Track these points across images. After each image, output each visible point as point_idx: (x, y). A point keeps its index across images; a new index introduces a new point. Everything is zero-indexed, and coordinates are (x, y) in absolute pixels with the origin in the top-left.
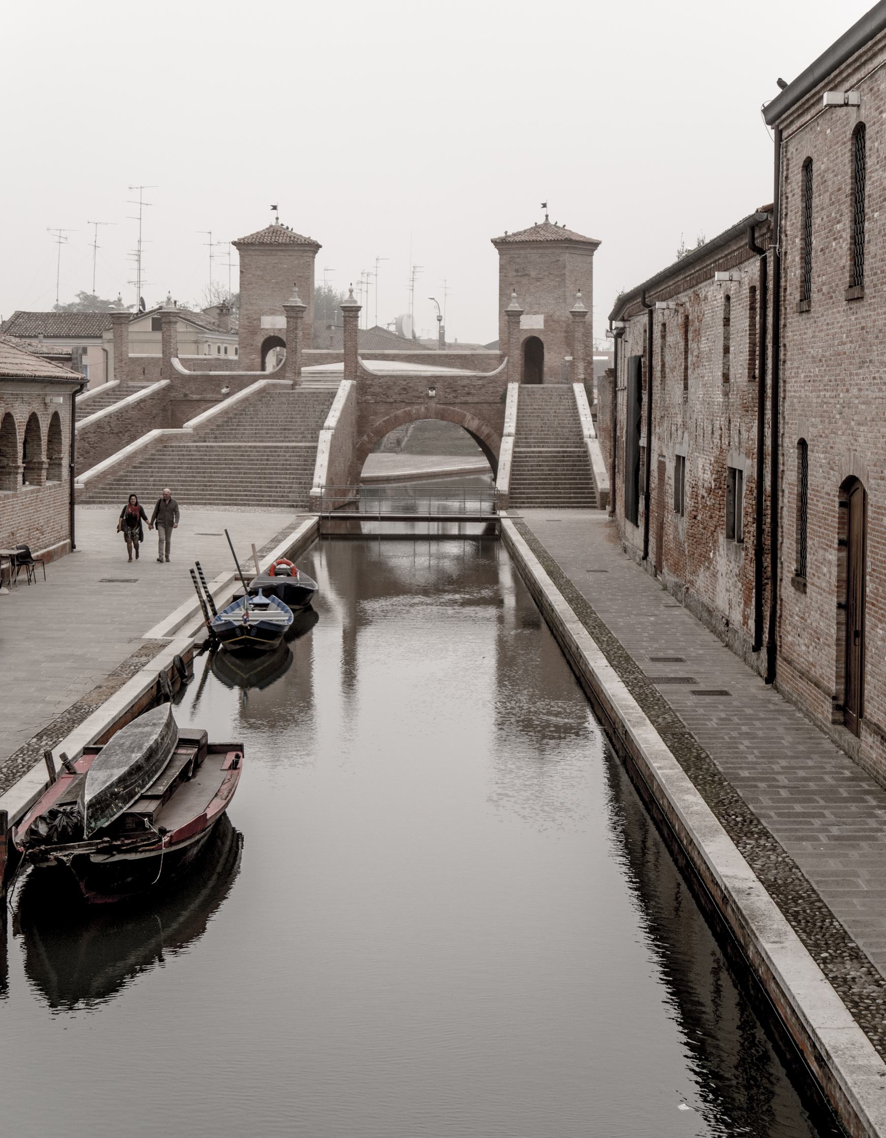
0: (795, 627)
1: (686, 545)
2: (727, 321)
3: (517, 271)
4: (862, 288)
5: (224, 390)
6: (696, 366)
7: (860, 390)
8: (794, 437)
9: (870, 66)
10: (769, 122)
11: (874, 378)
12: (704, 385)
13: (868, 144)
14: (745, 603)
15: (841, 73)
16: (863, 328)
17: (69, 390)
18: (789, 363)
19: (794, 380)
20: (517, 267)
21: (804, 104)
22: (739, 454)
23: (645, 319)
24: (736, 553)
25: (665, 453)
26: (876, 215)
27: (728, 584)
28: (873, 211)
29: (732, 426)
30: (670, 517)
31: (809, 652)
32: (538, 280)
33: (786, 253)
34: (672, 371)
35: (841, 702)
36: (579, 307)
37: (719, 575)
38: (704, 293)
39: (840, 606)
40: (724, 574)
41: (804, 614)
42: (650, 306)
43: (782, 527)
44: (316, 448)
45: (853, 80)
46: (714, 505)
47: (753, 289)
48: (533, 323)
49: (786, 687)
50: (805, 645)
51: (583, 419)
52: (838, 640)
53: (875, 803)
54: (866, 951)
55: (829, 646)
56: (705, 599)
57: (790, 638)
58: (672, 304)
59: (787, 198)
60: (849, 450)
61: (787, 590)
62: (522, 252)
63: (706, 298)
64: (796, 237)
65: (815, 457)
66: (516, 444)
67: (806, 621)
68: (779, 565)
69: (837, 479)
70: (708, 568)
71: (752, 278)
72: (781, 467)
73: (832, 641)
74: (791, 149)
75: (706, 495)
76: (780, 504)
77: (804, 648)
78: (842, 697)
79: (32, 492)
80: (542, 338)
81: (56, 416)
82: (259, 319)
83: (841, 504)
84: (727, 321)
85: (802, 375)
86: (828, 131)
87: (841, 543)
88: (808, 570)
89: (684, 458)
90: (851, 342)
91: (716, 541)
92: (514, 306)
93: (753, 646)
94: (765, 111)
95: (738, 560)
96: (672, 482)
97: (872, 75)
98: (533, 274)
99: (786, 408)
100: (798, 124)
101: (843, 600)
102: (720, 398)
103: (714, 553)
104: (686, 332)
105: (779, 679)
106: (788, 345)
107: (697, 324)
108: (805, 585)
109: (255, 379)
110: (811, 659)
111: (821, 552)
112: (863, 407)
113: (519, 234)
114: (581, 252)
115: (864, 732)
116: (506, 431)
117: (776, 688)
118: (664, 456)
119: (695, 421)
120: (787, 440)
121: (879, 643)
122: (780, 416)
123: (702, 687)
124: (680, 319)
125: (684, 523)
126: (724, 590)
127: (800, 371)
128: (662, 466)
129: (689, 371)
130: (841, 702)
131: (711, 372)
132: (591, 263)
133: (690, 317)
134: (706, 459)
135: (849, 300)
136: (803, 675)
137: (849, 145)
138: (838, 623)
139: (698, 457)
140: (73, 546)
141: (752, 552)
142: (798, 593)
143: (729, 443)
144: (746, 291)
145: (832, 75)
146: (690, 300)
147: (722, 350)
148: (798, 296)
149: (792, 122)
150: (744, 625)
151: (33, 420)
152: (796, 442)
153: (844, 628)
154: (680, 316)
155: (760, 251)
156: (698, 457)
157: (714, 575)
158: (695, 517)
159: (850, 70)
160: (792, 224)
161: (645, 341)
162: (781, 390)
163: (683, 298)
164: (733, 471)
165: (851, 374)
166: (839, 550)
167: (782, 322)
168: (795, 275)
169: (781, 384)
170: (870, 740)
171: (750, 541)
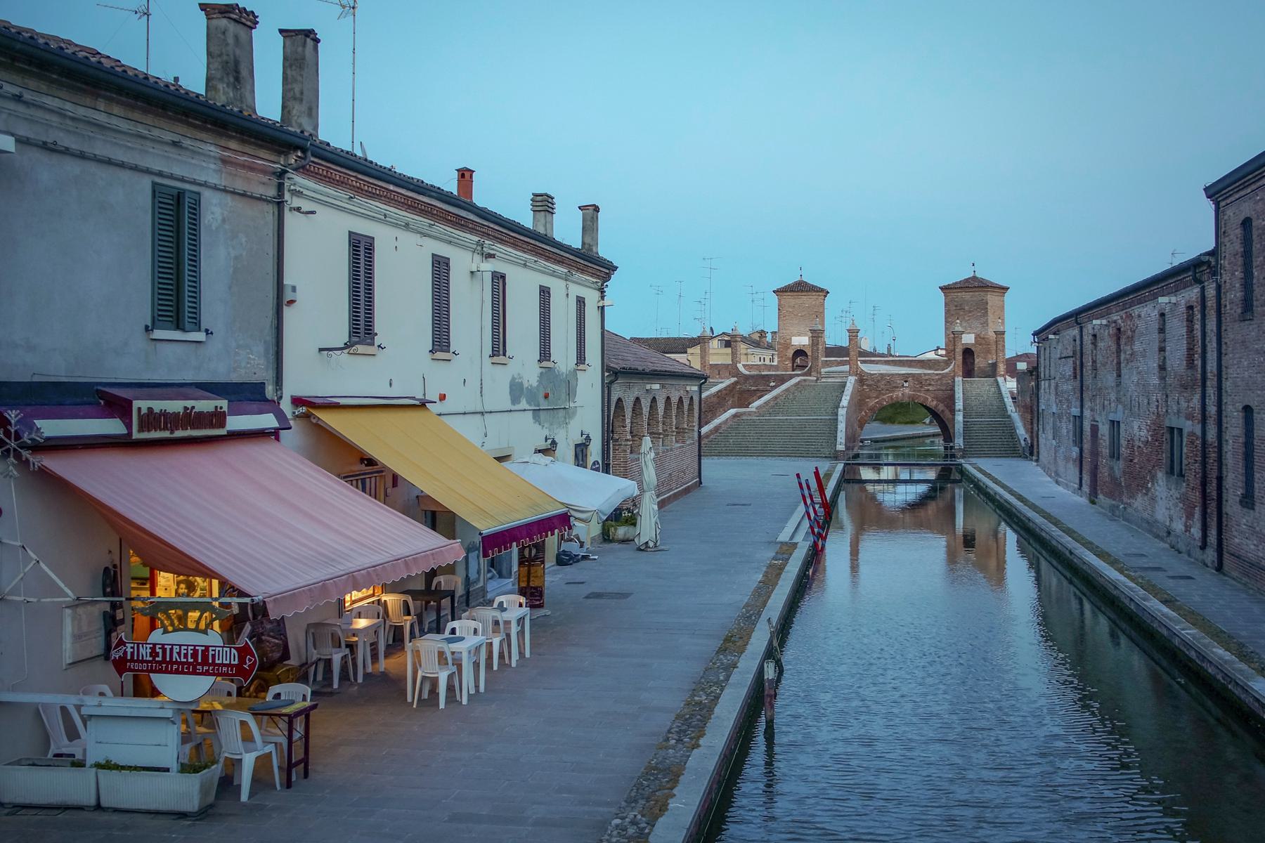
1: (1122, 479)
2: (1162, 330)
3: (956, 306)
5: (772, 384)
6: (1128, 361)
8: (1237, 404)
14: (1188, 518)
19: (1236, 366)
20: (956, 303)
21: (1245, 182)
22: (1178, 418)
24: (1177, 483)
25: (1097, 419)
27: (1167, 505)
29: (1170, 399)
30: (1104, 461)
31: (1259, 550)
32: (970, 312)
33: (1225, 282)
34: (1104, 365)
37: (1158, 499)
38: (1137, 313)
40: (1164, 498)
41: (1252, 524)
42: (1081, 324)
43: (1227, 465)
44: (837, 419)
46: (1151, 452)
47: (1190, 308)
48: (968, 339)
50: (1254, 545)
56: (1145, 515)
57: (1237, 540)
58: (1104, 322)
59: (1225, 245)
61: (1232, 505)
62: (959, 294)
63: (1139, 316)
64: (1237, 271)
67: (1255, 528)
68: (1224, 491)
70: (1146, 494)
71: (1189, 301)
74: (1230, 212)
75: (1142, 446)
77: (1252, 547)
79: (680, 447)
81: (692, 398)
84: (1162, 330)
85: (1246, 363)
88: (1256, 494)
89: (1118, 422)
91: (1153, 478)
92: (958, 328)
93: (1200, 547)
94: (1206, 189)
95: (1179, 488)
96: (1107, 438)
98: (966, 308)
99: (1227, 385)
100: (1237, 196)
103: (1153, 484)
104: (1119, 339)
106: (1229, 343)
107: (1129, 333)
108: (1253, 504)
109: (791, 377)
110: (1261, 555)
113: (956, 283)
114: (997, 294)
117: (1224, 575)
118: (1097, 421)
119: (1129, 397)
120: (1230, 407)
122: (1223, 391)
123: (1171, 574)
124: (1112, 331)
125: (1119, 466)
126: (1164, 510)
127: (1243, 360)
128: (1095, 429)
129: (1123, 365)
131: (1147, 365)
132: (1003, 301)
133: (1122, 329)
134: (1141, 422)
136: (1252, 565)
139: (1133, 421)
140: (701, 483)
142: (1245, 510)
143: (1167, 411)
144: (1182, 308)
146: (1122, 318)
147: (1157, 349)
148: (1239, 311)
150: (1186, 531)
151: (681, 399)
152: (1241, 407)
154: (1111, 329)
155: (1198, 281)
156: (1133, 421)
157: (1153, 499)
158: (1131, 461)
162: (1224, 373)
163: (1115, 317)
164: (1171, 429)
168: (1235, 296)
169: (1224, 369)
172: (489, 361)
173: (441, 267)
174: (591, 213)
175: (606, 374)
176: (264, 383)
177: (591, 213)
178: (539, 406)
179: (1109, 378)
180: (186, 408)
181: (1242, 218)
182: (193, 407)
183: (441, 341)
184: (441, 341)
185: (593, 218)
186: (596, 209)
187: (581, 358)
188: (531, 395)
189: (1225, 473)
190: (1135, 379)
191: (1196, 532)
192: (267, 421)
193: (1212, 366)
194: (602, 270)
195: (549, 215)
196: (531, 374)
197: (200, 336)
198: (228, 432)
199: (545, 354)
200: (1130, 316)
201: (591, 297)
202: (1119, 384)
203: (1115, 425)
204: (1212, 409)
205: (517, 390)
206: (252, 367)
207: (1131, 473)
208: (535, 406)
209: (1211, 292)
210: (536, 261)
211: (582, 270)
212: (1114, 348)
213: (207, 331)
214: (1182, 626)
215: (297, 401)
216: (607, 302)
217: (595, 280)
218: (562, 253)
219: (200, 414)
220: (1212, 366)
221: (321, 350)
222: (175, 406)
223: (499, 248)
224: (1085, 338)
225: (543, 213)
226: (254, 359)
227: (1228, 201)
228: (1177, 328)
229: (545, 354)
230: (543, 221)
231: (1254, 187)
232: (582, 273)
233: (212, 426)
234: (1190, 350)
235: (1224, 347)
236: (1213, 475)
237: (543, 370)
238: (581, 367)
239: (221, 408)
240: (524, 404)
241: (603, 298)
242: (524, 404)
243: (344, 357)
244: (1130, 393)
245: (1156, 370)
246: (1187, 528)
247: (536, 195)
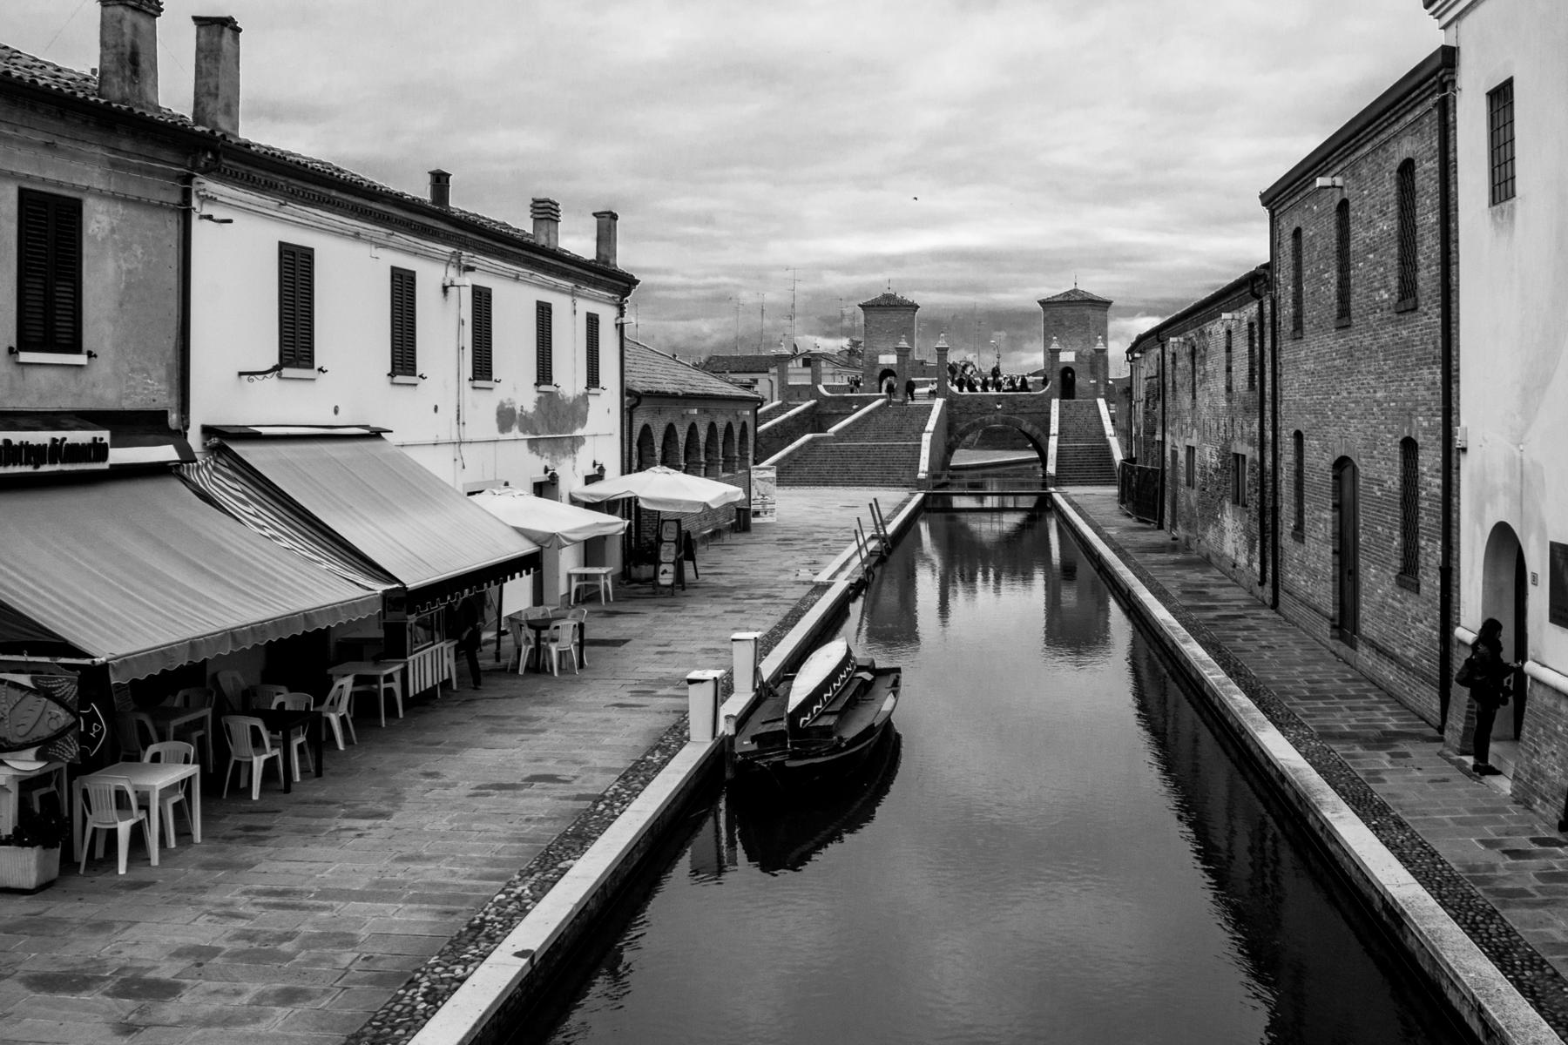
0: (1294, 567)
2: (1229, 349)
4: (1350, 319)
5: (855, 407)
6: (1202, 382)
7: (1350, 393)
9: (1353, 158)
10: (1263, 205)
11: (1363, 384)
12: (1210, 395)
13: (1352, 214)
15: (1327, 164)
16: (1351, 348)
17: (752, 406)
18: (1284, 376)
23: (1158, 351)
26: (1360, 265)
28: (1358, 262)
32: (1070, 328)
34: (1182, 386)
35: (1337, 623)
36: (1100, 345)
37: (1226, 531)
39: (1334, 552)
44: (920, 445)
45: (1338, 169)
47: (1251, 325)
48: (1067, 357)
49: (1288, 612)
51: (1105, 423)
52: (1334, 577)
53: (1376, 699)
54: (1406, 819)
55: (1326, 582)
57: (1290, 576)
58: (1181, 339)
60: (1341, 437)
61: (1286, 540)
63: (1210, 333)
65: (1311, 443)
66: (1059, 442)
69: (1329, 459)
70: (1217, 526)
72: (1280, 452)
73: (1329, 577)
74: (1284, 223)
76: (1280, 478)
77: (1303, 583)
78: (1337, 618)
80: (1074, 368)
81: (744, 424)
82: (877, 358)
83: (1334, 477)
84: (1229, 349)
85: (1297, 385)
86: (1315, 208)
87: (1334, 505)
88: (1306, 525)
89: (1193, 448)
90: (1341, 358)
91: (1223, 507)
92: (1055, 346)
96: (1184, 465)
97: (1353, 165)
98: (1067, 323)
99: (1282, 408)
101: (1337, 548)
102: (1223, 403)
104: (1193, 358)
105: (1281, 605)
107: (1203, 352)
108: (1303, 537)
109: (876, 398)
110: (1310, 591)
111: (1317, 513)
112: (1353, 405)
115: (1360, 645)
116: (1052, 432)
117: (1278, 612)
121: (1373, 579)
124: (1188, 350)
125: (1194, 494)
128: (1175, 454)
129: (1197, 386)
130: (1337, 623)
135: (1338, 328)
136: (1303, 602)
137: (1334, 217)
138: (1334, 565)
141: (1255, 514)
144: (1245, 326)
145: (1320, 167)
148: (1291, 328)
149: (1283, 204)
151: (729, 427)
153: (1337, 568)
155: (1257, 296)
157: (1222, 531)
158: (1204, 490)
159: (1335, 162)
160: (1284, 276)
161: (1158, 366)
162: (1279, 395)
163: (1191, 334)
164: (1237, 456)
165: (1341, 382)
166: (1333, 511)
167: (1278, 347)
169: (1279, 391)
170: (1366, 651)
171: (1253, 506)
172: (467, 385)
173: (403, 284)
174: (607, 221)
175: (626, 399)
176: (166, 412)
177: (607, 221)
178: (536, 434)
179: (1186, 401)
180: (54, 440)
181: (1294, 228)
182: (64, 439)
183: (404, 360)
184: (404, 360)
185: (609, 226)
186: (614, 217)
187: (593, 380)
188: (527, 424)
189: (1280, 504)
190: (1207, 401)
191: (1257, 566)
192: (166, 453)
193: (1268, 388)
194: (620, 285)
195: (552, 226)
196: (526, 398)
197: (81, 359)
198: (111, 466)
199: (544, 373)
200: (1202, 333)
201: (607, 315)
202: (1194, 407)
203: (1190, 450)
204: (1269, 434)
205: (506, 418)
206: (152, 393)
207: (1203, 503)
208: (532, 433)
209: (1267, 309)
210: (531, 275)
211: (596, 284)
212: (1190, 367)
213: (90, 354)
214: (1212, 670)
215: (208, 431)
216: (625, 320)
217: (611, 295)
218: (565, 266)
219: (74, 447)
220: (1268, 388)
221: (241, 374)
222: (41, 437)
223: (481, 260)
224: (1167, 356)
225: (545, 221)
226: (153, 385)
227: (1282, 210)
228: (1241, 347)
229: (544, 373)
230: (545, 230)
231: (1301, 194)
232: (595, 288)
233: (89, 460)
234: (1252, 370)
235: (1278, 366)
236: (1269, 505)
237: (543, 395)
238: (593, 390)
239: (101, 439)
240: (516, 432)
241: (622, 315)
242: (516, 432)
243: (272, 380)
244: (1202, 417)
245: (1223, 392)
246: (1250, 562)
247: (536, 201)
